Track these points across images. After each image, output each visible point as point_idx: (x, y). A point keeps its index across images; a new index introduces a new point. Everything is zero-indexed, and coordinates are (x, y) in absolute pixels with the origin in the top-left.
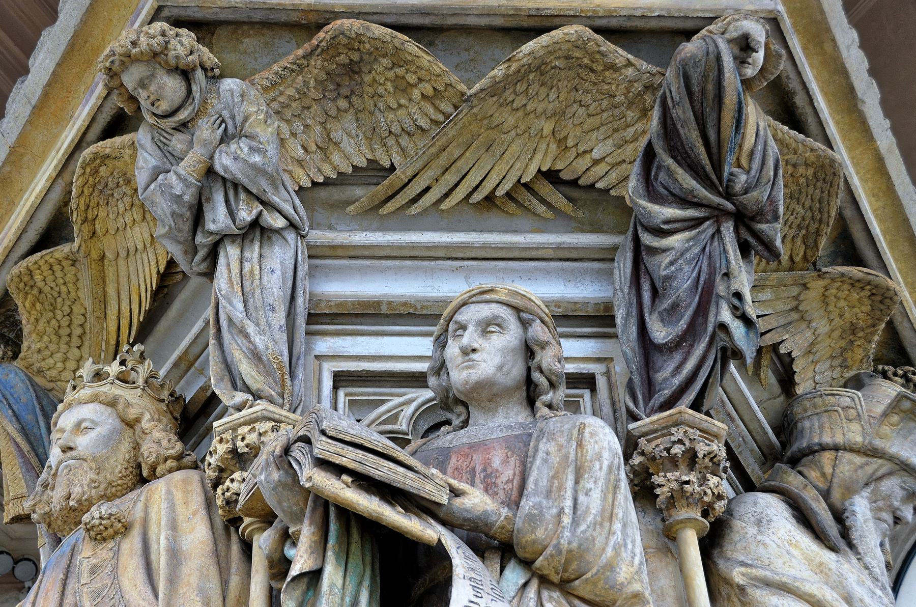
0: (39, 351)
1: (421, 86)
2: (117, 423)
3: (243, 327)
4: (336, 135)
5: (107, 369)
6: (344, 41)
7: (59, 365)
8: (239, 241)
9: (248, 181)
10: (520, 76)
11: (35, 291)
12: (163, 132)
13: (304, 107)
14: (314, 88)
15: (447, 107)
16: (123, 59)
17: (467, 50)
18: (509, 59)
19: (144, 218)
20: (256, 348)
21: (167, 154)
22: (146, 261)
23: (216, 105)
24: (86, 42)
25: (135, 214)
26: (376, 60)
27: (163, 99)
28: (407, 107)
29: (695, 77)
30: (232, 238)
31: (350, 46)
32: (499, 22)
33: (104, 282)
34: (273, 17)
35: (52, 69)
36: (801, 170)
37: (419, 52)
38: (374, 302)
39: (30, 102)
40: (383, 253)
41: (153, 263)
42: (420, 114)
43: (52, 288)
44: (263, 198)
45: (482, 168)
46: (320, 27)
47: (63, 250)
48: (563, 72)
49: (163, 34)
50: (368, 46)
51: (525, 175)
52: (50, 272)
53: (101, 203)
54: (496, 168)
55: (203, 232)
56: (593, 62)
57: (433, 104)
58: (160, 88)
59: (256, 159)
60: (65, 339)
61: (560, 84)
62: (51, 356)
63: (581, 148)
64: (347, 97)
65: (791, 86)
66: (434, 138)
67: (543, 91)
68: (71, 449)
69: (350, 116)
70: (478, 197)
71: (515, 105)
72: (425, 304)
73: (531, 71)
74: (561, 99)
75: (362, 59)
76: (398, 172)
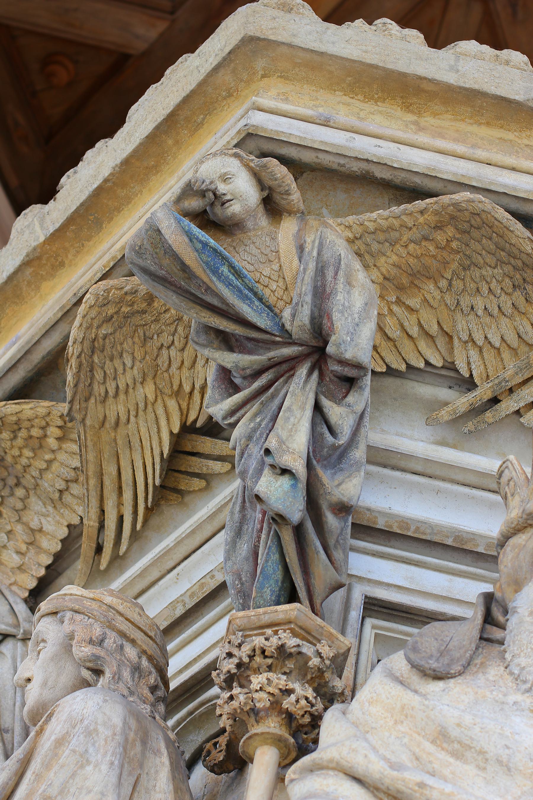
4: (34, 524)
29: (149, 263)
36: (440, 237)
37: (17, 408)
48: (118, 333)
51: (163, 448)
56: (132, 305)
61: (125, 345)
63: (197, 386)
65: (355, 169)
67: (117, 363)
69: (33, 499)
73: (91, 357)
76: (85, 521)
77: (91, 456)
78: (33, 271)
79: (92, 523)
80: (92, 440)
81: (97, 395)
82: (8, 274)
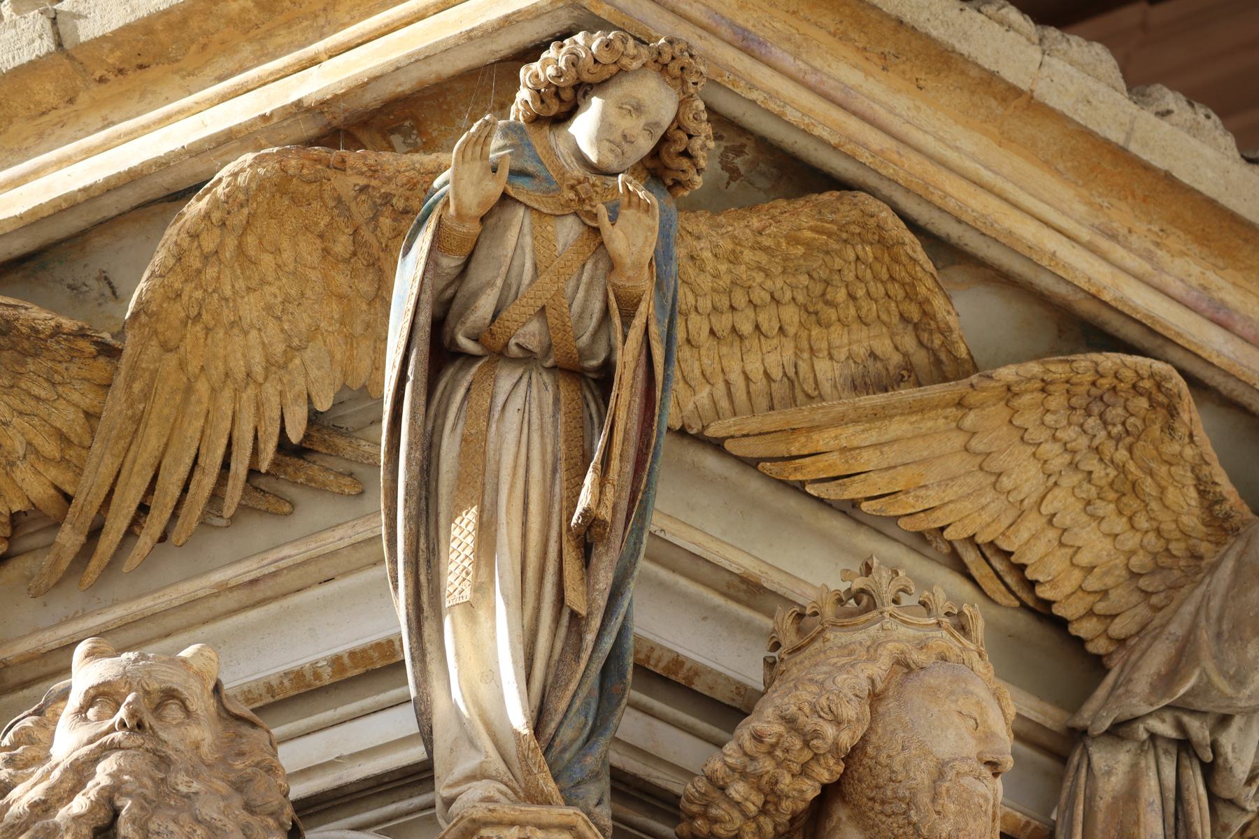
11: (836, 246)
35: (1201, 188)
41: (986, 517)
60: (724, 302)
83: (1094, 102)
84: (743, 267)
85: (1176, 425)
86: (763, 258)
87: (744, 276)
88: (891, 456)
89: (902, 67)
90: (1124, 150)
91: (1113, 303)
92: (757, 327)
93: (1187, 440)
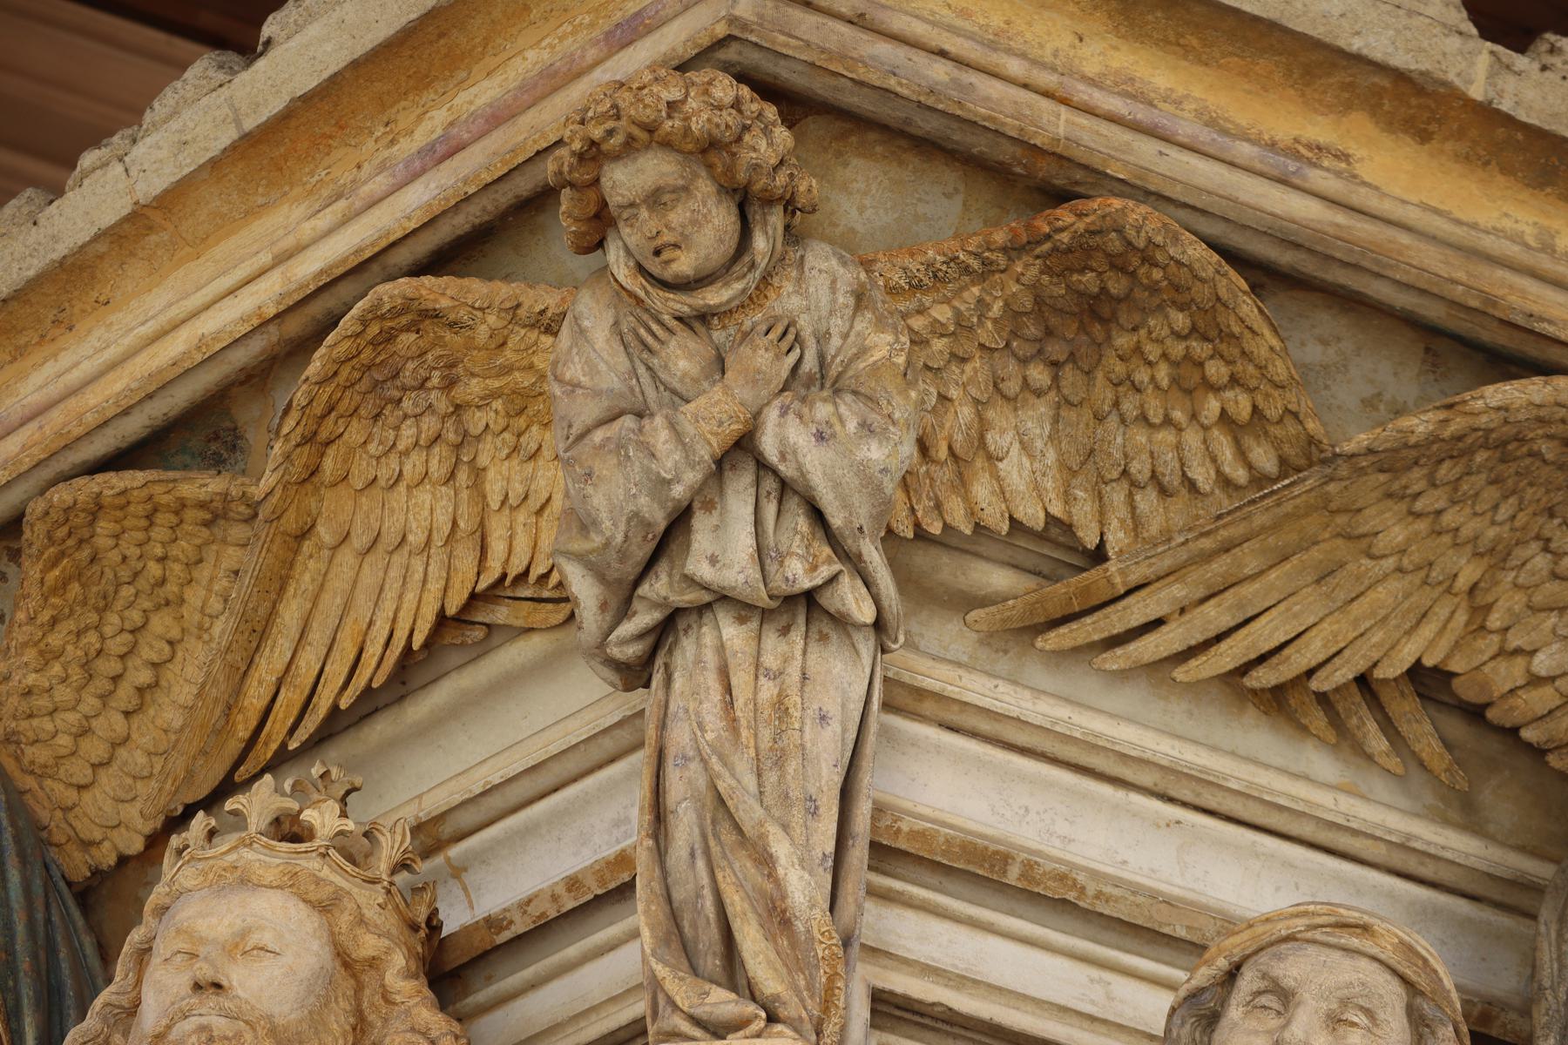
0: (28, 693)
1: (1229, 394)
2: (327, 954)
3: (763, 837)
5: (309, 815)
6: (1114, 243)
7: (64, 740)
8: (754, 624)
9: (831, 496)
10: (1456, 449)
11: (85, 553)
12: (645, 317)
13: (953, 355)
14: (995, 321)
15: (1264, 457)
16: (636, 132)
17: (1324, 342)
18: (1450, 407)
19: (452, 476)
20: (784, 897)
21: (642, 370)
22: (418, 576)
23: (787, 300)
24: (442, 35)
25: (434, 463)
26: (1160, 308)
27: (689, 249)
28: (1181, 430)
30: (742, 608)
31: (1119, 262)
32: (1433, 312)
33: (282, 589)
34: (958, 136)
38: (997, 852)
39: (238, 122)
40: (1022, 738)
41: (435, 587)
42: (1204, 454)
43: (125, 558)
44: (849, 543)
45: (1295, 616)
46: (1061, 197)
47: (204, 485)
48: (1548, 469)
49: (737, 105)
50: (1157, 274)
51: (1386, 662)
52: (144, 523)
53: (363, 412)
54: (1325, 625)
55: (670, 575)
57: (1237, 443)
58: (694, 222)
59: (875, 452)
61: (1530, 491)
62: (51, 714)
63: (1514, 641)
64: (1055, 365)
66: (1219, 517)
67: (1491, 494)
68: (218, 986)
69: (1043, 408)
70: (1264, 677)
71: (1419, 505)
72: (1108, 890)
74: (1517, 524)
75: (1127, 297)
76: (1112, 567)
77: (1260, 519)
78: (1383, 88)
79: (1118, 580)
80: (1296, 507)
81: (1404, 481)
82: (1365, 52)
83: (189, 137)
84: (69, 648)
85: (452, 317)
86: (71, 625)
87: (79, 653)
88: (319, 637)
89: (76, 310)
90: (246, 137)
91: (282, 308)
92: (155, 665)
93: (479, 314)
